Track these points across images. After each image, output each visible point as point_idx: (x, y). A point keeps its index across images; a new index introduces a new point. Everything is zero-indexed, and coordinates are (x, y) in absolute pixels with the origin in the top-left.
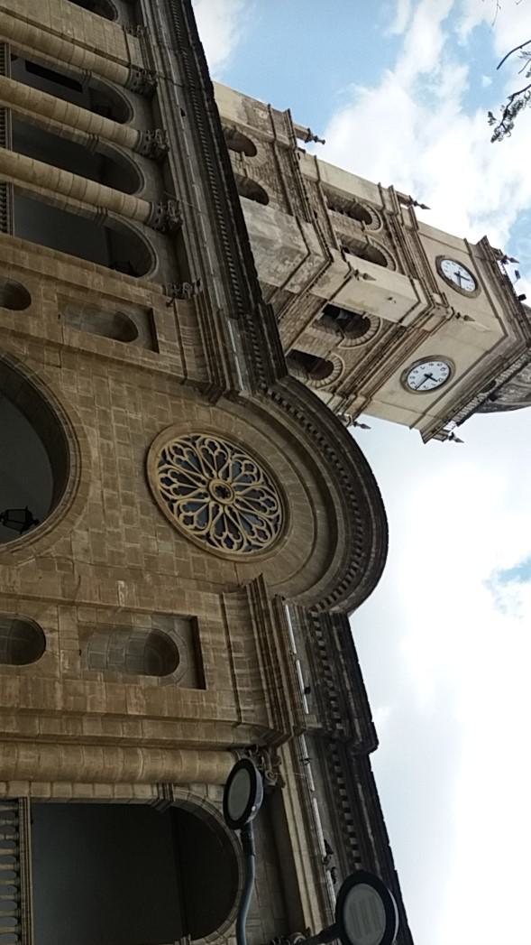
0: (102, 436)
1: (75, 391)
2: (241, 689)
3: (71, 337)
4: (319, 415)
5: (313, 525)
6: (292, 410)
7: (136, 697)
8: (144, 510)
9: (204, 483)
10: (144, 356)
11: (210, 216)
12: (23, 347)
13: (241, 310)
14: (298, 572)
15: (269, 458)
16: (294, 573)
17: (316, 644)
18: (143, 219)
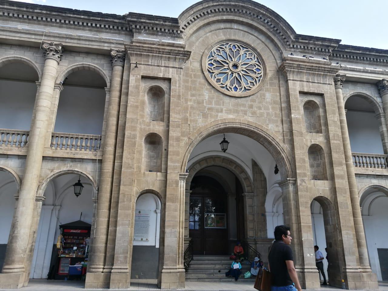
0: (222, 111)
1: (201, 120)
2: (322, 81)
3: (175, 118)
4: (195, 10)
5: (242, 32)
6: (190, 22)
7: (331, 117)
8: (254, 101)
9: (232, 73)
10: (176, 86)
11: (45, 25)
12: (184, 140)
13: (124, 29)
14: (266, 45)
15: (212, 41)
16: (266, 46)
17: (302, 49)
18: (57, 64)
